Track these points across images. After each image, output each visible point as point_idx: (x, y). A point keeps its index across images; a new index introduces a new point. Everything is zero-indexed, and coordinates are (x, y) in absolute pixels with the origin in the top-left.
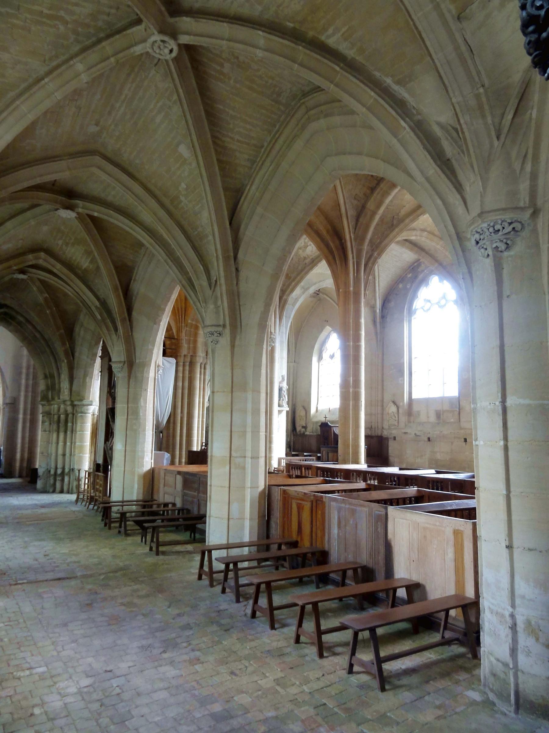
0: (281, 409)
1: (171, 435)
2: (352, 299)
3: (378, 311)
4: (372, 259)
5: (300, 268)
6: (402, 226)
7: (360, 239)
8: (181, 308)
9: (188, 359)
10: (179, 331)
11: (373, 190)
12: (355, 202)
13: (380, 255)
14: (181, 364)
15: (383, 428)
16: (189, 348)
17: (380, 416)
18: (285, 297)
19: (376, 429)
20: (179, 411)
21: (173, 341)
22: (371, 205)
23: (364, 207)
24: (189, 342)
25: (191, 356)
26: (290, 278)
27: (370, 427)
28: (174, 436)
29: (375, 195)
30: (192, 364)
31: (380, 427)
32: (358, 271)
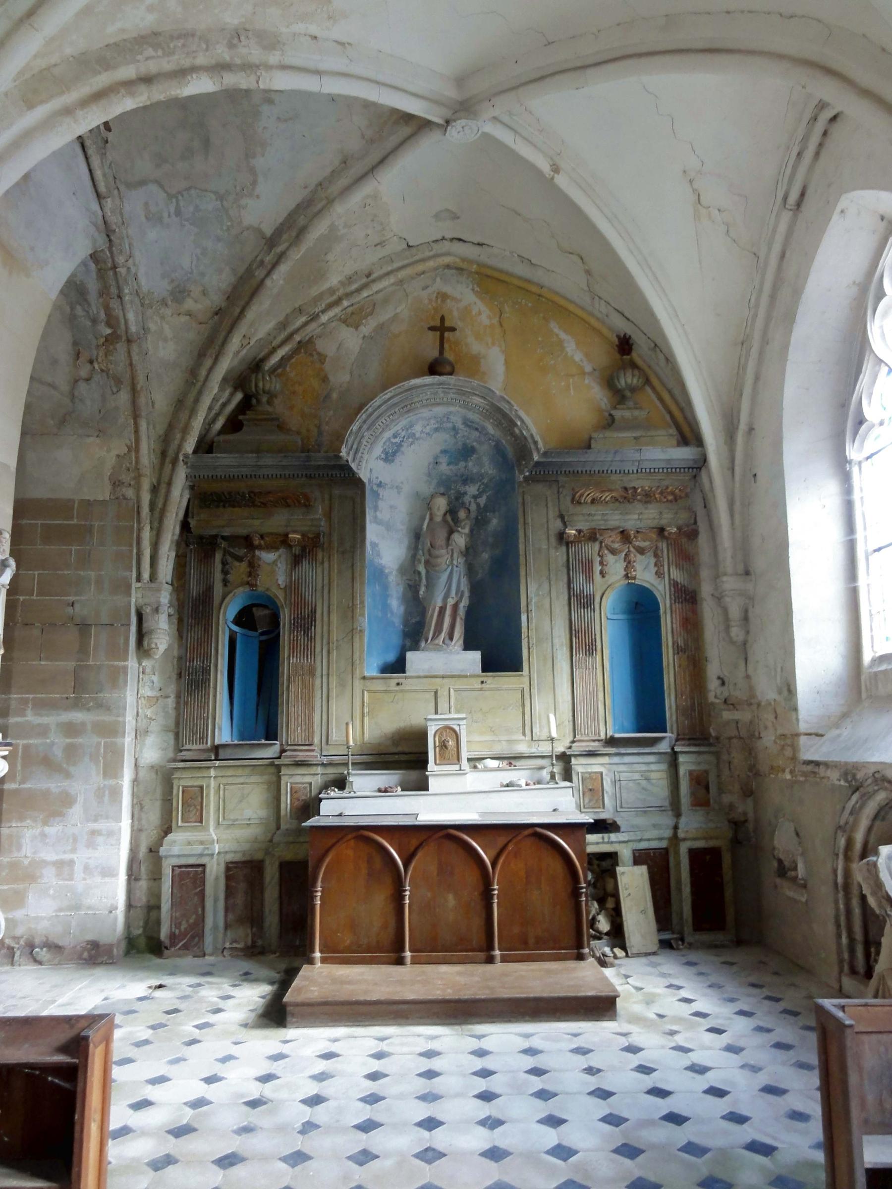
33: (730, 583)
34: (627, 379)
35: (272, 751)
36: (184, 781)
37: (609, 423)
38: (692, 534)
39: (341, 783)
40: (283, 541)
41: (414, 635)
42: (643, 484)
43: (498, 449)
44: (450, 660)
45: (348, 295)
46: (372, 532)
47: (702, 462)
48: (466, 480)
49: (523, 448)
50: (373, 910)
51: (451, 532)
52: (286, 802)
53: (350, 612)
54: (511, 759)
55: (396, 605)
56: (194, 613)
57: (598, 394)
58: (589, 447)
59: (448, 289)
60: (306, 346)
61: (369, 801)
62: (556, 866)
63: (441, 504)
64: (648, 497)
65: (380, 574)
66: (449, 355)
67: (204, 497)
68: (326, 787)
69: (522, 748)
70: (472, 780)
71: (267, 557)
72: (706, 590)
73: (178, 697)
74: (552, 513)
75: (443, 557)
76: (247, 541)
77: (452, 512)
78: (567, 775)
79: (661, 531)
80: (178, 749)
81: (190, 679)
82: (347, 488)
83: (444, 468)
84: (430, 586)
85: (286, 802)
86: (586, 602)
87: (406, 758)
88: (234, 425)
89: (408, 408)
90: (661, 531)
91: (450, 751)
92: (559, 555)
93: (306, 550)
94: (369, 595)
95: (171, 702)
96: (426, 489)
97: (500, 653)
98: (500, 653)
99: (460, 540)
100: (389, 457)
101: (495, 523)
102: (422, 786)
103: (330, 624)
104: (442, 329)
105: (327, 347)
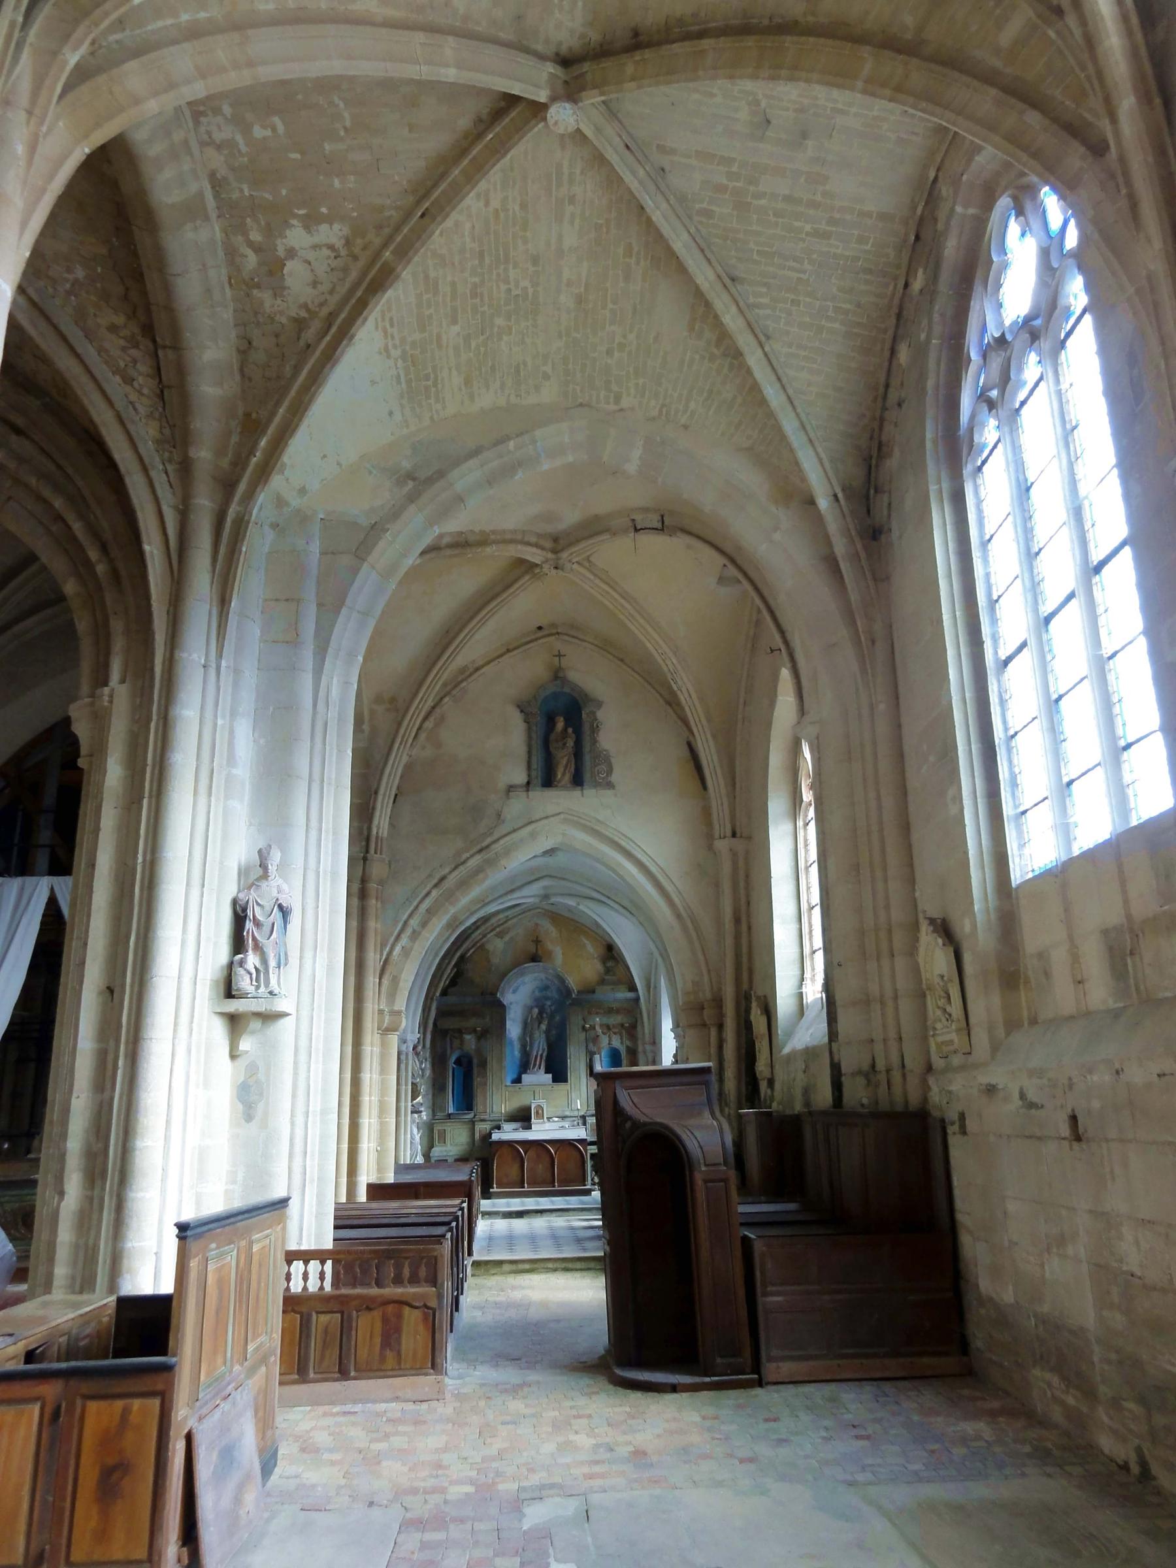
0: (233, 1006)
3: (823, 503)
5: (288, 370)
15: (929, 1068)
17: (906, 1007)
19: (896, 1076)
27: (866, 1066)
31: (913, 1063)
33: (648, 1048)
34: (610, 964)
35: (471, 1116)
36: (437, 1128)
37: (602, 982)
38: (634, 1026)
39: (499, 1128)
40: (475, 1031)
41: (525, 1066)
42: (615, 1006)
43: (559, 991)
44: (539, 1077)
45: (499, 926)
46: (509, 1024)
47: (637, 999)
48: (547, 998)
49: (568, 992)
50: (514, 1171)
51: (540, 1023)
52: (477, 1136)
53: (501, 1060)
54: (563, 1118)
55: (517, 1053)
56: (438, 1061)
57: (599, 967)
58: (593, 992)
59: (539, 922)
60: (482, 947)
61: (510, 1133)
62: (575, 1154)
63: (536, 1011)
64: (618, 1011)
65: (511, 1043)
66: (540, 952)
67: (442, 1014)
68: (493, 1129)
69: (567, 1113)
70: (547, 1126)
71: (467, 1037)
72: (640, 1049)
73: (434, 1095)
74: (580, 1017)
75: (537, 1035)
76: (460, 1032)
77: (540, 1013)
78: (584, 1124)
79: (622, 1025)
80: (434, 1114)
81: (438, 1087)
82: (500, 1009)
83: (537, 993)
84: (532, 1045)
85: (477, 1136)
86: (590, 1055)
87: (523, 1117)
88: (453, 982)
89: (522, 974)
90: (622, 1025)
91: (540, 1115)
92: (583, 1036)
93: (482, 1035)
94: (508, 1051)
95: (430, 1096)
96: (529, 1002)
97: (559, 1074)
98: (559, 1074)
99: (543, 1027)
100: (514, 992)
101: (558, 1018)
102: (529, 1127)
103: (492, 1064)
104: (537, 941)
105: (490, 947)
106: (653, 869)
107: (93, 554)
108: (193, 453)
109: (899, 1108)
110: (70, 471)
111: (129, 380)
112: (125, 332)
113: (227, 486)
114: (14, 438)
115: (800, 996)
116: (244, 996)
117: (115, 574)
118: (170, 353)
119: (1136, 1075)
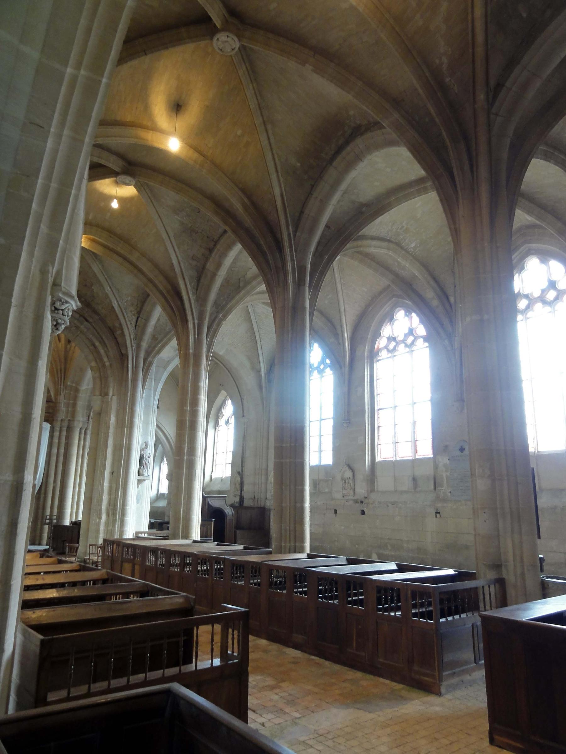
0: (141, 478)
1: (41, 505)
2: (191, 361)
3: (263, 375)
4: (217, 321)
6: (249, 287)
7: (202, 300)
8: (61, 370)
9: (66, 424)
10: (57, 394)
11: (211, 251)
12: (194, 263)
13: (225, 317)
14: (58, 429)
15: (266, 499)
16: (67, 412)
18: (149, 359)
20: (51, 480)
21: (51, 404)
22: (210, 266)
23: (204, 267)
24: (67, 405)
25: (69, 420)
26: (157, 339)
28: (44, 508)
29: (213, 255)
30: (70, 429)
32: (200, 333)
106: (167, 434)
107: (105, 359)
108: (142, 343)
109: (259, 506)
110: (104, 337)
111: (131, 324)
112: (133, 312)
113: (148, 353)
114: (86, 323)
115: (211, 476)
116: (143, 475)
117: (111, 365)
118: (143, 320)
119: (319, 503)
